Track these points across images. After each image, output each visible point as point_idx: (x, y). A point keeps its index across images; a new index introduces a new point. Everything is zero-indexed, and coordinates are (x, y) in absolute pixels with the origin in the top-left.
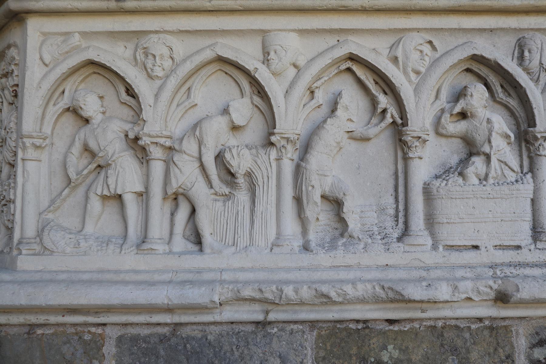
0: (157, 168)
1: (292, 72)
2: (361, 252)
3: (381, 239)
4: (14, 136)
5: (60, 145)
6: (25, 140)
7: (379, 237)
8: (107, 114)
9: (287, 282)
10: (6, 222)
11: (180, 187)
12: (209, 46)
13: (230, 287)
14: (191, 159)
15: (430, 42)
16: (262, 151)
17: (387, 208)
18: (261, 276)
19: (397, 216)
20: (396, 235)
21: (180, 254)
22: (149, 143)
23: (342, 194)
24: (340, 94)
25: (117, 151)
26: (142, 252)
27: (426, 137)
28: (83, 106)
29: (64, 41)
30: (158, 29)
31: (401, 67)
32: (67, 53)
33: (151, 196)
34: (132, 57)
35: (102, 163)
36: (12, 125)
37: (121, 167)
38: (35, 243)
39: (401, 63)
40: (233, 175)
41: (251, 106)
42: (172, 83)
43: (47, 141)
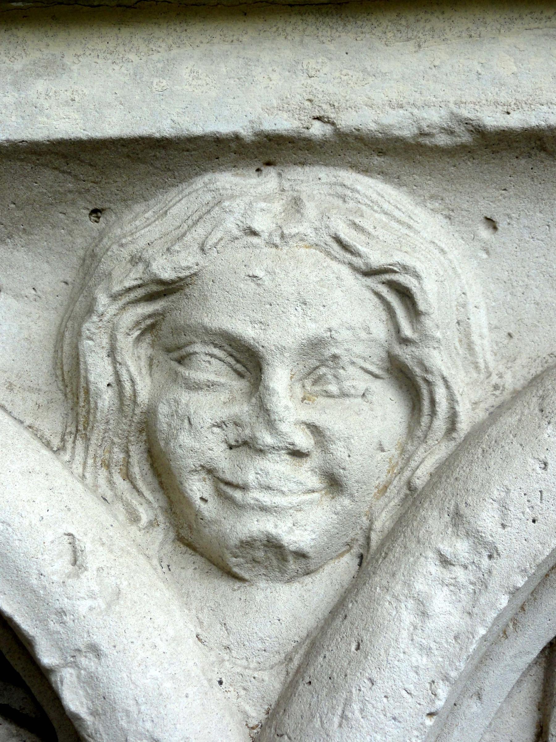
30: (283, 123)
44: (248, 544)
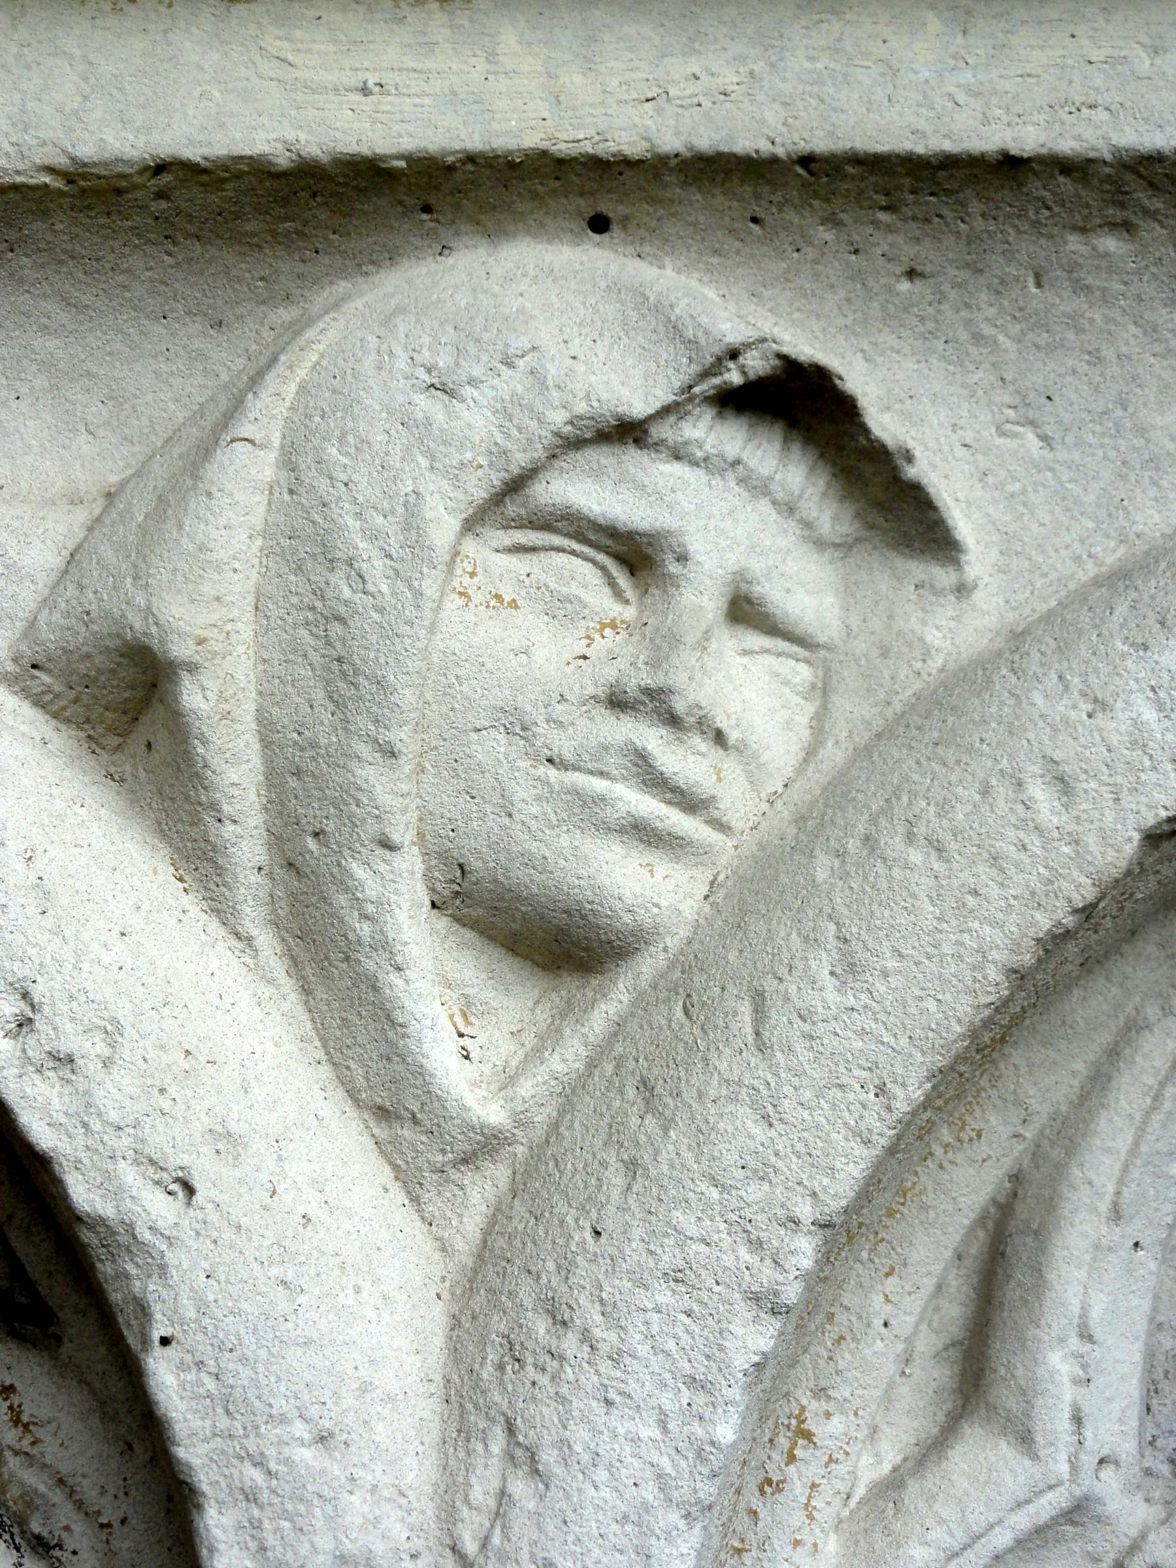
15: (798, 402)
31: (246, 843)
39: (237, 770)
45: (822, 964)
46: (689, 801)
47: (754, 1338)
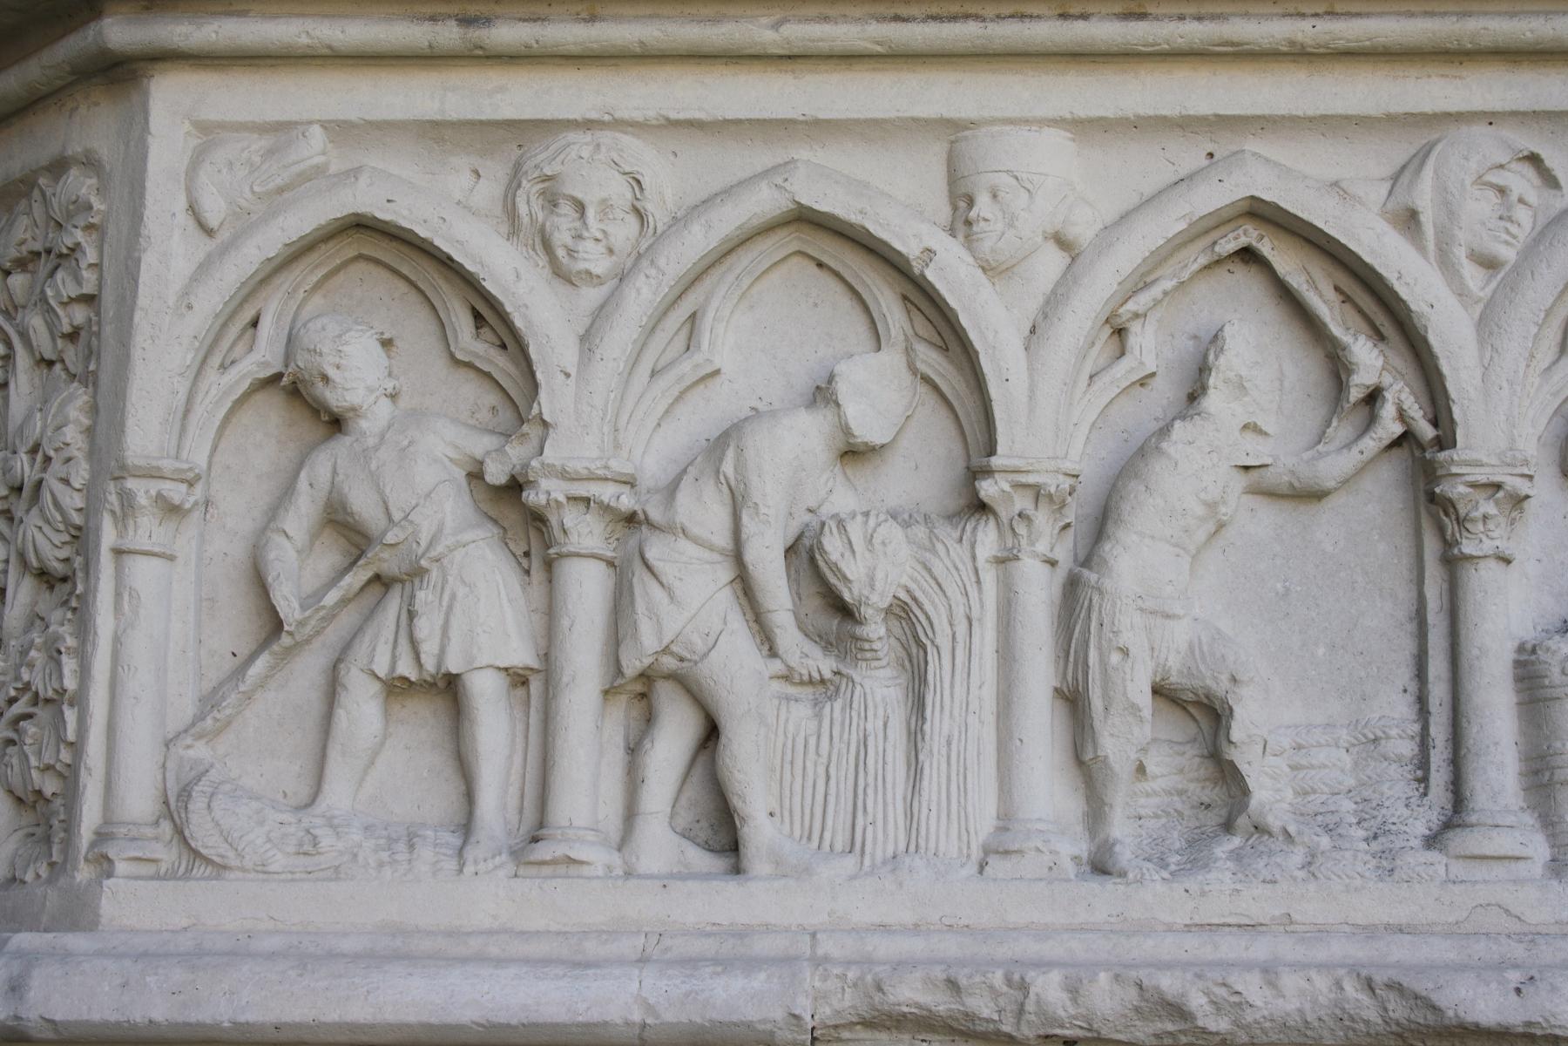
0: (586, 587)
1: (1051, 263)
2: (1295, 879)
3: (1366, 840)
4: (81, 474)
5: (237, 507)
6: (131, 484)
7: (1361, 833)
8: (403, 403)
9: (1043, 965)
10: (34, 773)
11: (666, 650)
12: (766, 173)
13: (851, 975)
14: (707, 555)
15: (1534, 159)
16: (947, 533)
17: (1388, 737)
18: (950, 947)
19: (1423, 763)
20: (1420, 828)
21: (666, 880)
22: (562, 498)
23: (1224, 678)
24: (1216, 338)
25: (449, 524)
26: (533, 870)
27: (1523, 487)
28: (331, 372)
29: (270, 153)
30: (594, 115)
31: (1431, 245)
32: (280, 190)
33: (565, 679)
34: (498, 210)
35: (390, 564)
36: (72, 434)
37: (463, 582)
38: (156, 839)
40: (844, 610)
41: (906, 377)
42: (643, 295)
43: (199, 489)
44: (579, 272)
45: (1544, 265)
46: (1515, 237)
47: (1534, 330)
